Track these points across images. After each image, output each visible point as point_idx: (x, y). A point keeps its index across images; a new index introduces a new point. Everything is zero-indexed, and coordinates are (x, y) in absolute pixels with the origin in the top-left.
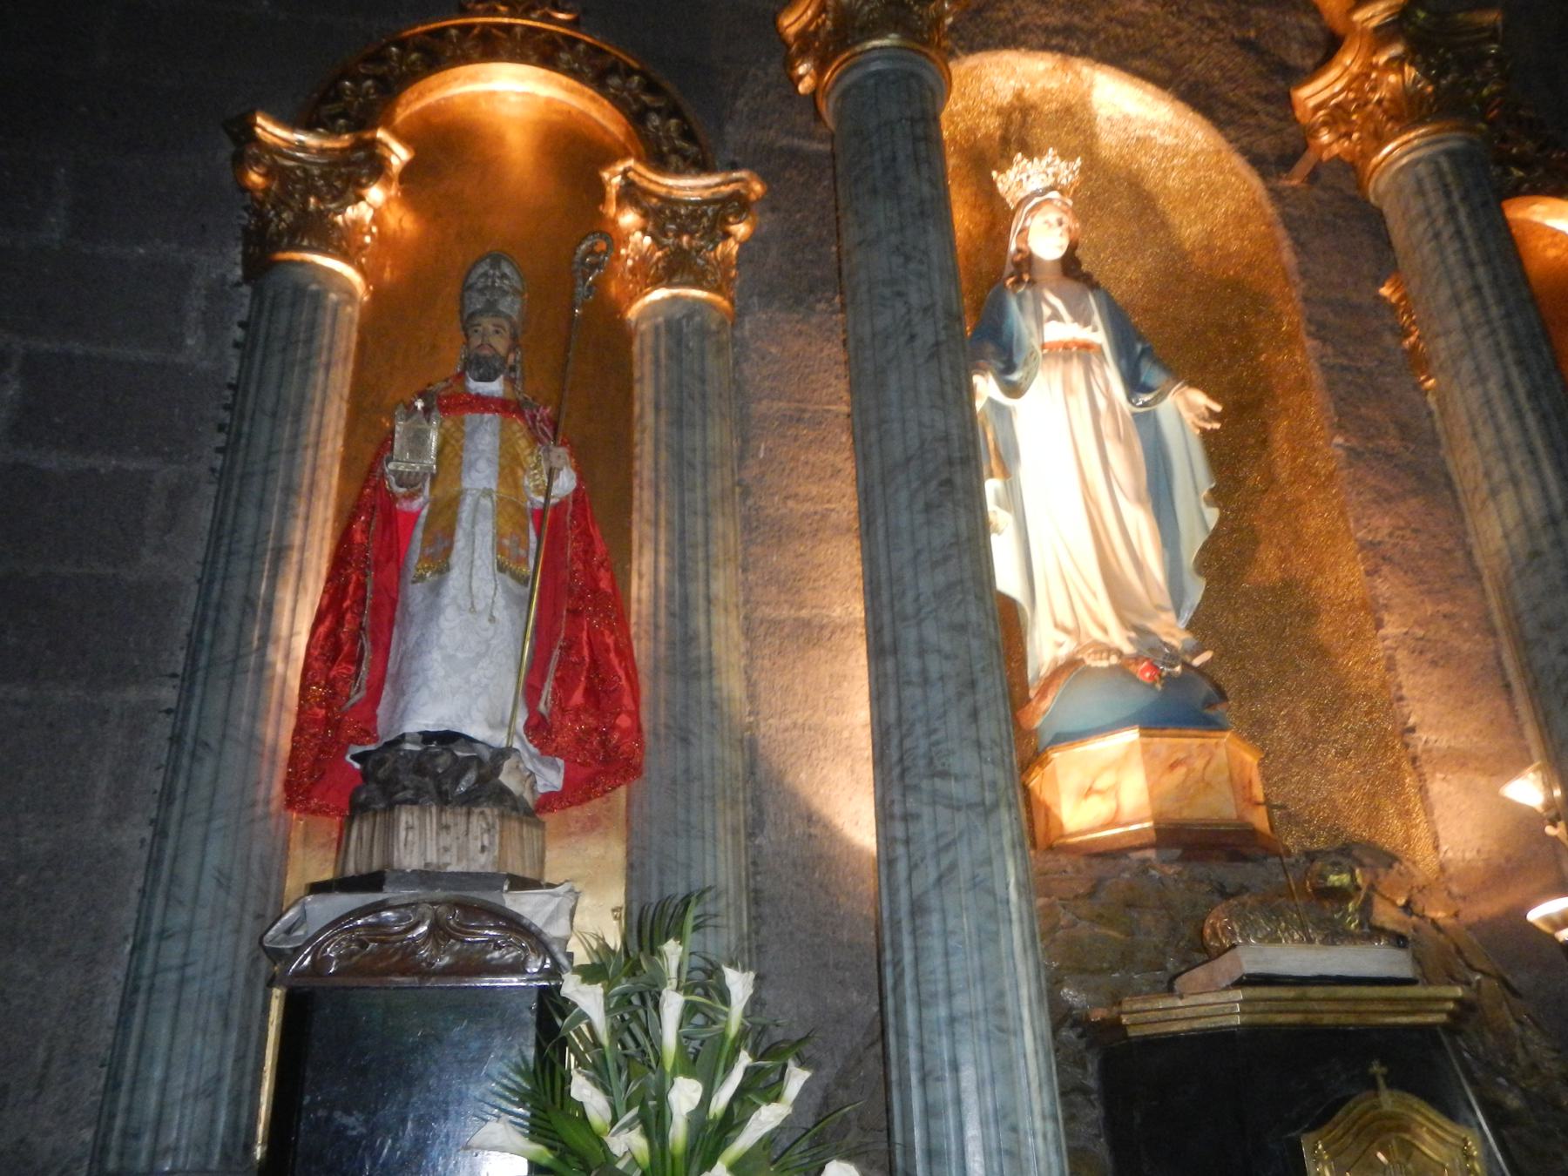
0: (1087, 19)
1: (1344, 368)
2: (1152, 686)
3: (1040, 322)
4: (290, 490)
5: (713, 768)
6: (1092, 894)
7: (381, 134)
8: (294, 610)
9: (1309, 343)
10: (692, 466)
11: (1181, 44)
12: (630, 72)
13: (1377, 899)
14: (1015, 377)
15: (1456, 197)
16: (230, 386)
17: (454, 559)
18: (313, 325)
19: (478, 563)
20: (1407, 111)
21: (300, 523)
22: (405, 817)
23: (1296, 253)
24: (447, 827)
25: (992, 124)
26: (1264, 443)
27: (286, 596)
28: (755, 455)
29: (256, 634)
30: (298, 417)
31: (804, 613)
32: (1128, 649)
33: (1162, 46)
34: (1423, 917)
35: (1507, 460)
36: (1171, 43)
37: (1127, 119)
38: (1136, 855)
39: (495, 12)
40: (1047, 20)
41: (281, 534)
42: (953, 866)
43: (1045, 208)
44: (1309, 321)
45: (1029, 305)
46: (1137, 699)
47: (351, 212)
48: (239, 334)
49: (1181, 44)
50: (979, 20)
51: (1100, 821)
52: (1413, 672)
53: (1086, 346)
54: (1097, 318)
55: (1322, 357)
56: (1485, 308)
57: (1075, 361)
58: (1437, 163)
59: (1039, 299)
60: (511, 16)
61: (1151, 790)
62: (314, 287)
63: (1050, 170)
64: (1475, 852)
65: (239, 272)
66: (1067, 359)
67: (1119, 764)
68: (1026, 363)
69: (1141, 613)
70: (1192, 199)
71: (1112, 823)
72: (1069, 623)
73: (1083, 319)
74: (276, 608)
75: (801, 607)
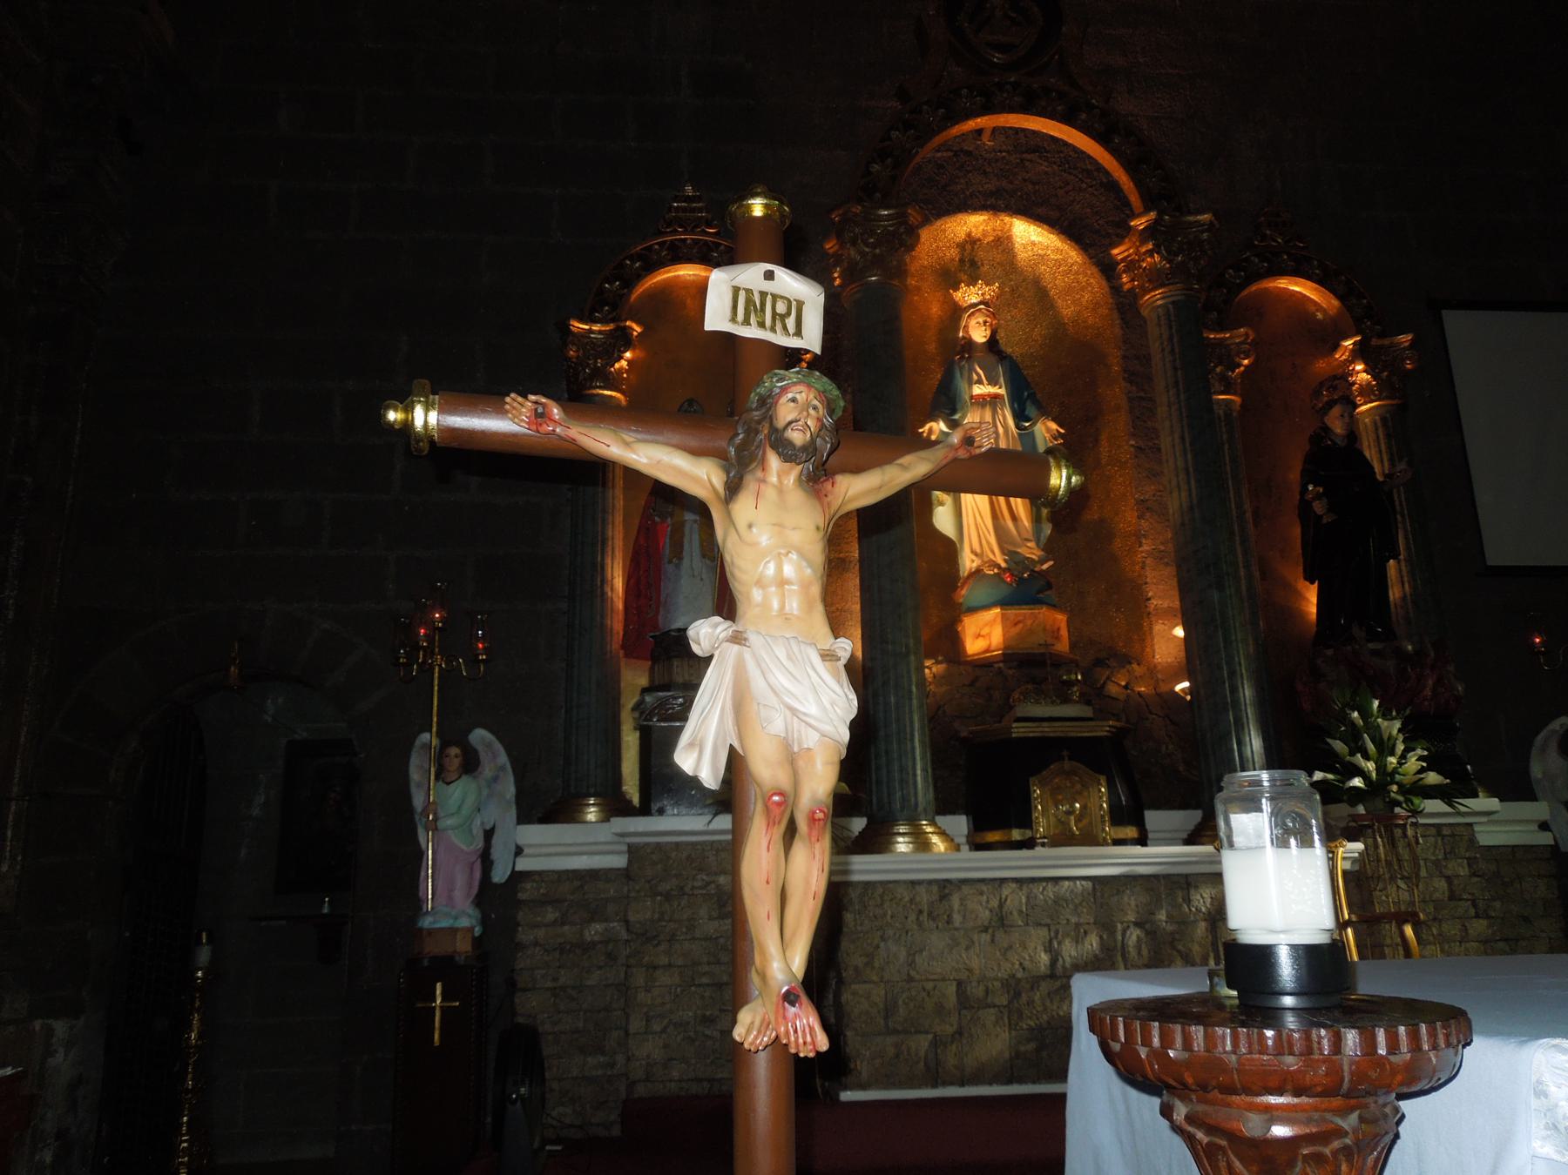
0: (1011, 183)
1: (1142, 398)
2: (1011, 585)
3: (971, 383)
4: (604, 511)
6: (972, 684)
7: (628, 323)
8: (612, 568)
9: (1124, 384)
11: (1067, 193)
13: (1109, 682)
14: (956, 417)
15: (1174, 330)
17: (684, 553)
19: (694, 554)
20: (1156, 279)
21: (610, 526)
22: (676, 663)
23: (1122, 328)
24: (692, 667)
25: (953, 253)
26: (1097, 441)
27: (608, 561)
29: (599, 579)
31: (841, 555)
32: (1003, 565)
33: (1056, 195)
34: (1133, 690)
35: (1177, 476)
36: (1061, 192)
37: (1033, 244)
38: (996, 666)
39: (675, 232)
40: (986, 186)
41: (603, 533)
43: (977, 314)
44: (1125, 371)
45: (966, 374)
46: (1003, 591)
47: (617, 366)
49: (1067, 193)
50: (945, 193)
51: (982, 650)
52: (1154, 570)
53: (996, 397)
54: (1002, 380)
55: (1130, 392)
56: (1178, 395)
57: (988, 407)
58: (1168, 310)
59: (972, 370)
61: (1004, 635)
63: (980, 292)
64: (1174, 659)
66: (983, 406)
67: (991, 623)
68: (963, 408)
69: (1014, 544)
70: (1068, 290)
71: (987, 651)
72: (978, 550)
73: (993, 381)
74: (606, 567)
75: (840, 553)
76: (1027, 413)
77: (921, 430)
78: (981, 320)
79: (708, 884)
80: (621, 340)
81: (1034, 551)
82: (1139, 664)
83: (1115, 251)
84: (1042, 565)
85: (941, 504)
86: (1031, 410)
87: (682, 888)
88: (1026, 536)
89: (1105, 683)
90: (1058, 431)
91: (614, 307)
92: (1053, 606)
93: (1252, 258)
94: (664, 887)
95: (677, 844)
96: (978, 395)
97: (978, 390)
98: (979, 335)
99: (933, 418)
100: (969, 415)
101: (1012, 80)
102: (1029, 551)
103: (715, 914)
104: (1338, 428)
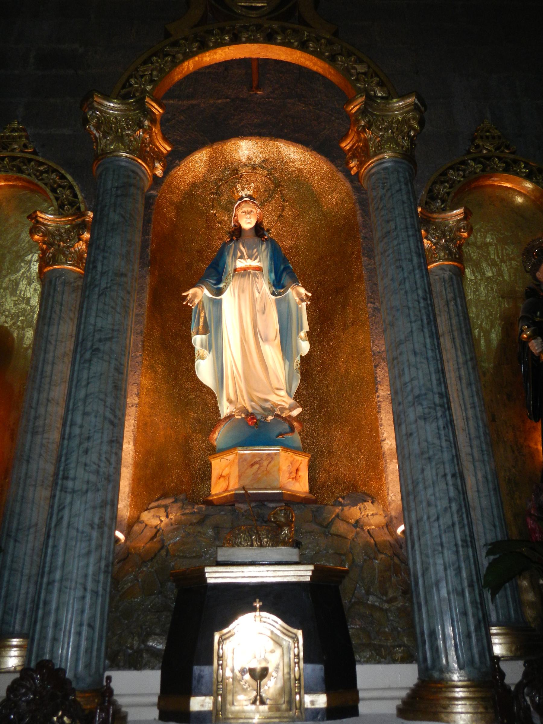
5: (37, 472)
6: (201, 522)
10: (50, 343)
12: (54, 171)
13: (337, 520)
23: (363, 217)
42: (62, 518)
71: (226, 490)
76: (282, 282)
81: (284, 399)
82: (372, 503)
83: (343, 145)
84: (291, 411)
88: (275, 384)
89: (332, 523)
90: (306, 295)
92: (295, 450)
93: (469, 161)
96: (241, 268)
97: (240, 264)
100: (231, 284)
102: (279, 398)
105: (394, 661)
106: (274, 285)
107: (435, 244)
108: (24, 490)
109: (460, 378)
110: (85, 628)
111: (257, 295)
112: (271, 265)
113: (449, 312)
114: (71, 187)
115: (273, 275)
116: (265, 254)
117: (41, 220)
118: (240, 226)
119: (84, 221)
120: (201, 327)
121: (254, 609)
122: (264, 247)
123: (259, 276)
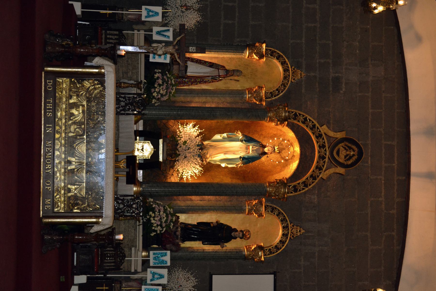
4: (218, 52)
7: (265, 58)
14: (244, 142)
16: (232, 44)
18: (239, 52)
21: (214, 53)
28: (227, 104)
30: (227, 52)
39: (292, 71)
40: (308, 153)
47: (254, 55)
48: (240, 44)
59: (256, 146)
60: (292, 73)
62: (244, 52)
65: (248, 43)
77: (239, 131)
78: (270, 149)
79: (130, 70)
80: (261, 56)
84: (205, 161)
85: (221, 136)
86: (245, 161)
87: (129, 64)
91: (272, 55)
94: (129, 61)
95: (139, 64)
97: (251, 147)
98: (266, 150)
99: (243, 135)
101: (327, 153)
103: (123, 71)
104: (237, 233)
105: (143, 179)
106: (243, 157)
107: (254, 206)
108: (183, 94)
109: (211, 206)
110: (152, 117)
111: (240, 152)
112: (250, 156)
113: (231, 207)
114: (278, 95)
115: (246, 157)
116: (254, 155)
117: (263, 88)
118: (266, 147)
119: (262, 101)
120: (229, 136)
121: (154, 149)
122: (257, 155)
123: (246, 153)
